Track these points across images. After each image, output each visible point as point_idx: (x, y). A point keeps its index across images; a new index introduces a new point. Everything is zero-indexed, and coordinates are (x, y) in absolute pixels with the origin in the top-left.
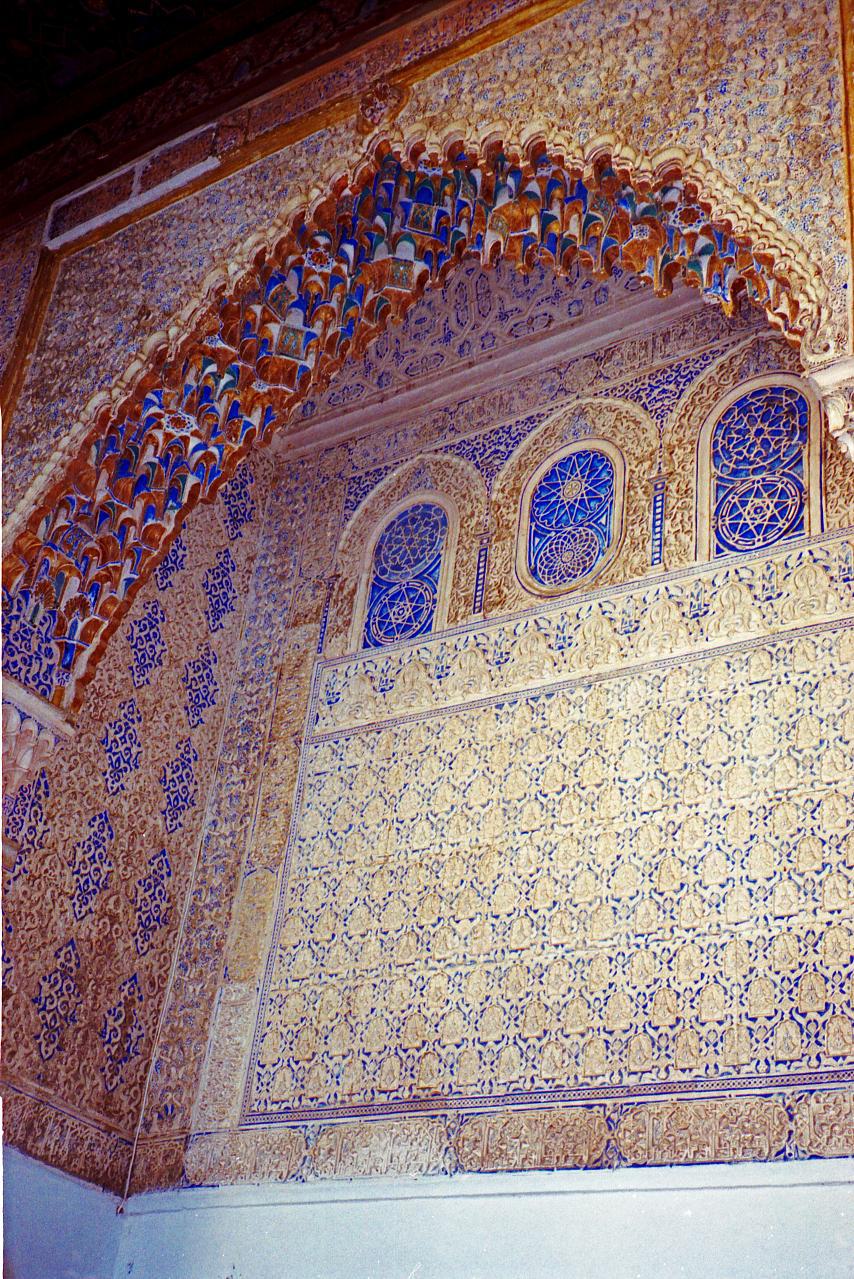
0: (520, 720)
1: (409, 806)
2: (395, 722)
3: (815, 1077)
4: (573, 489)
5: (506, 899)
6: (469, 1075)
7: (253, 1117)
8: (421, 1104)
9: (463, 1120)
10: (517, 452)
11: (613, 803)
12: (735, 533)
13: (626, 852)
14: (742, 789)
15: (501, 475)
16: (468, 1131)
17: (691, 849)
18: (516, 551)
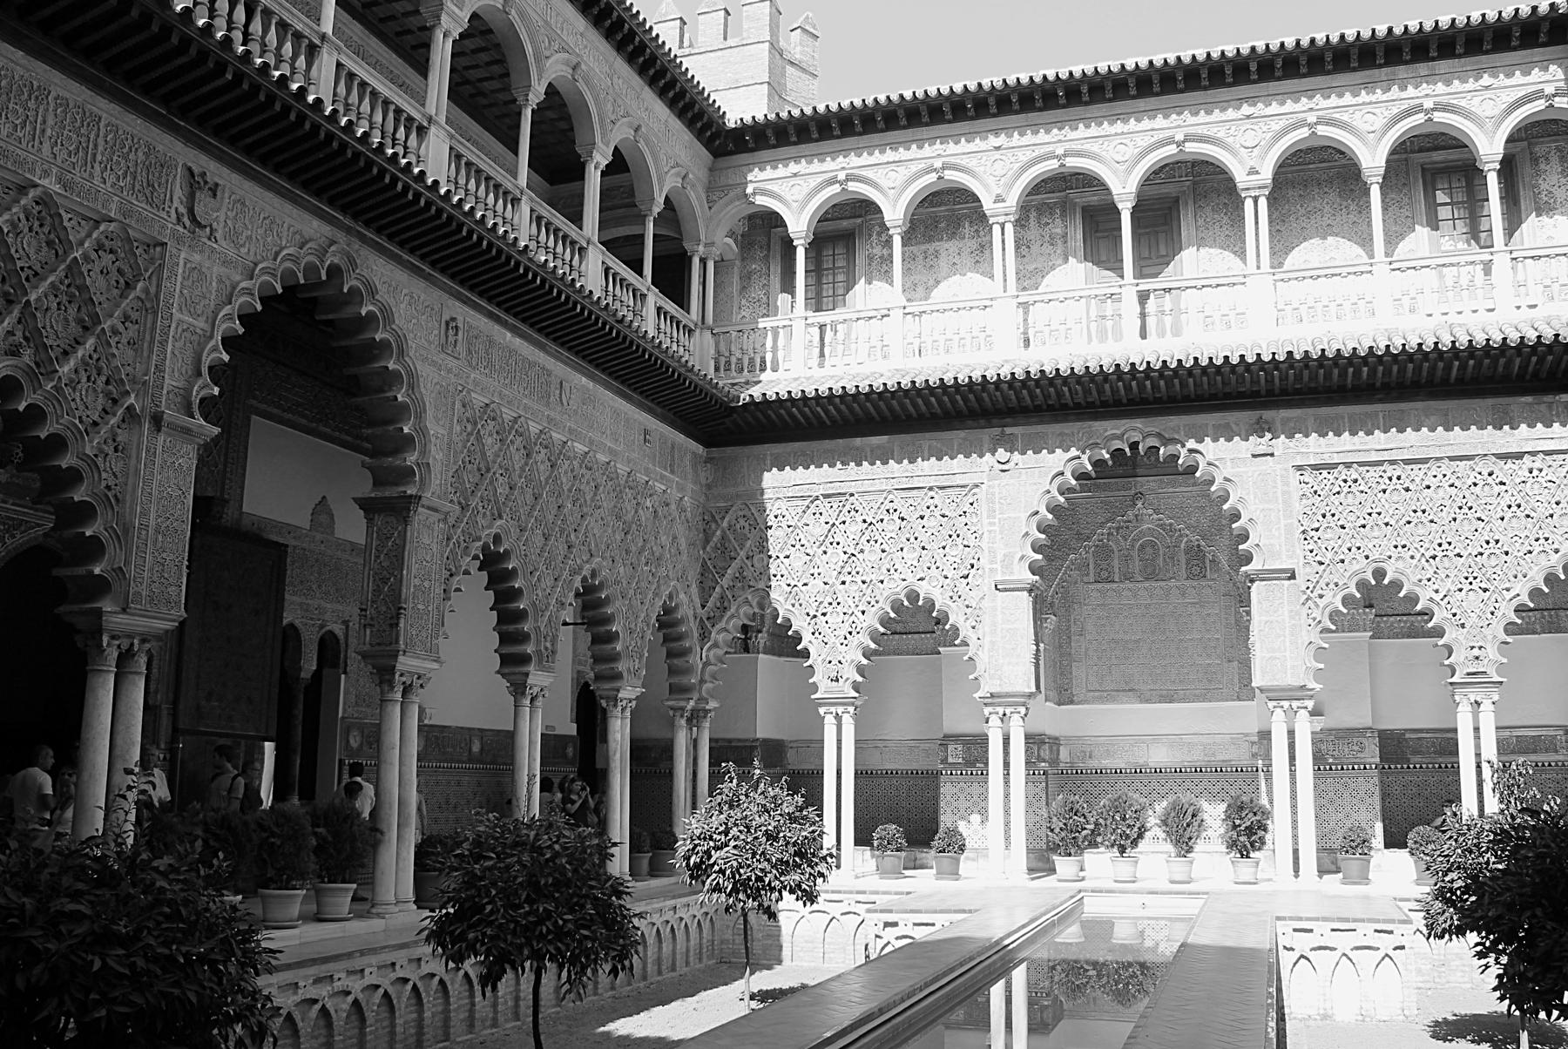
4: (1149, 550)
18: (1136, 565)
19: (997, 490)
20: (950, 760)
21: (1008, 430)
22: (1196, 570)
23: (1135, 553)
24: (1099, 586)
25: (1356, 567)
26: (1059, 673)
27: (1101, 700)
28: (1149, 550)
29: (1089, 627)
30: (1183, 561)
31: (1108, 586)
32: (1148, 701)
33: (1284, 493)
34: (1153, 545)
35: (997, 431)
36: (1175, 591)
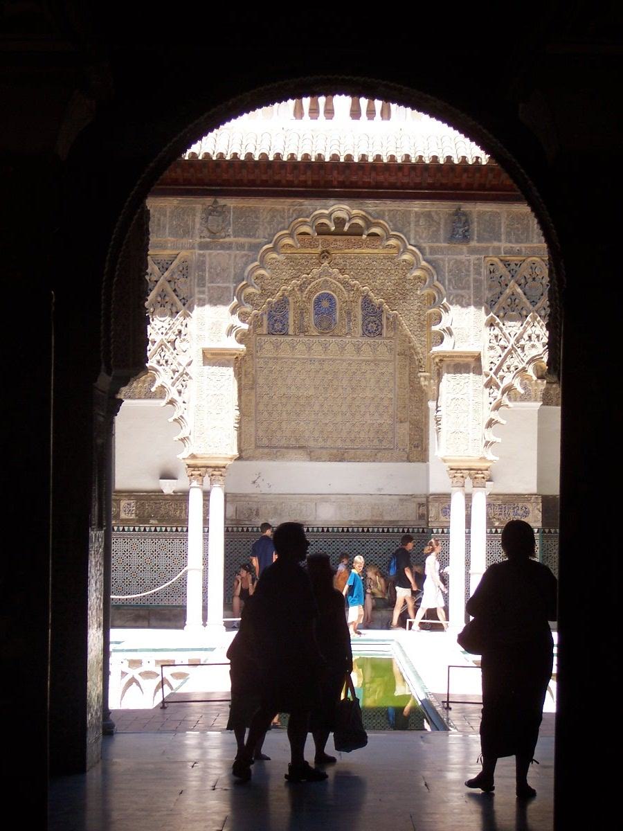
0: (317, 366)
1: (289, 381)
2: (282, 358)
3: (381, 449)
4: (325, 304)
5: (316, 408)
6: (312, 444)
7: (257, 447)
8: (300, 448)
9: (311, 452)
10: (309, 287)
11: (340, 390)
12: (367, 332)
13: (344, 402)
14: (368, 393)
15: (305, 293)
16: (312, 454)
17: (358, 403)
18: (310, 319)
19: (208, 259)
20: (123, 516)
21: (222, 201)
22: (372, 327)
23: (311, 307)
24: (274, 338)
25: (534, 352)
26: (260, 435)
27: (274, 457)
28: (325, 304)
29: (261, 381)
30: (360, 317)
31: (281, 339)
32: (318, 459)
33: (476, 281)
34: (330, 298)
35: (209, 200)
36: (349, 348)
